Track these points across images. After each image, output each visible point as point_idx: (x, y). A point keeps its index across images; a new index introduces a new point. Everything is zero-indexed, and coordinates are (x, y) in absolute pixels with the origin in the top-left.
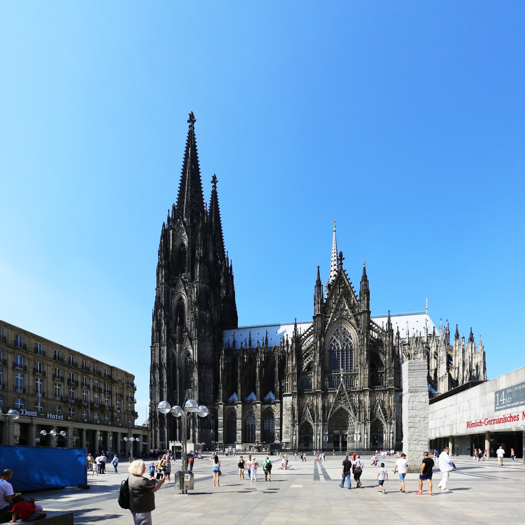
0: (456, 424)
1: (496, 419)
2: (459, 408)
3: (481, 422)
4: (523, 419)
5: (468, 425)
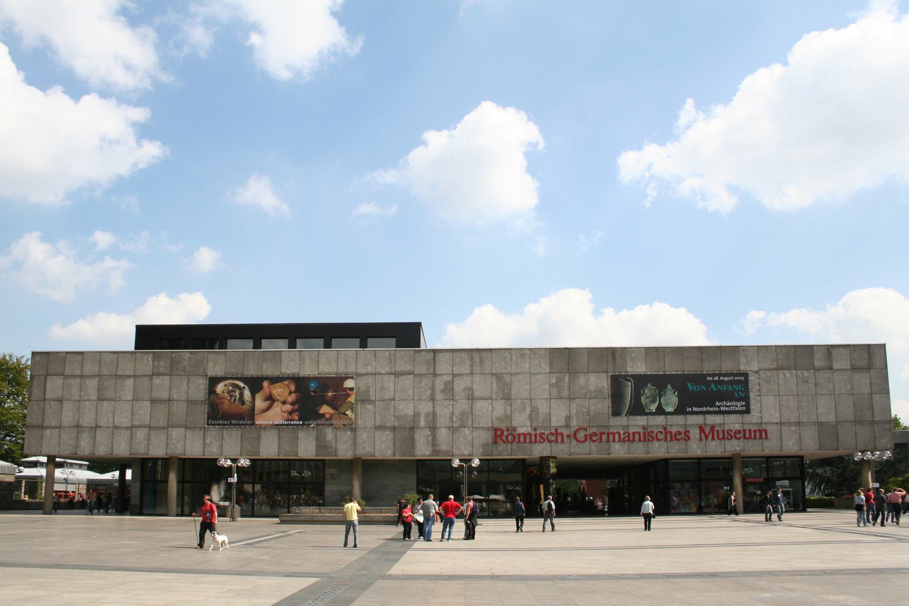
0: (433, 428)
1: (619, 434)
2: (449, 389)
3: (557, 433)
4: (701, 439)
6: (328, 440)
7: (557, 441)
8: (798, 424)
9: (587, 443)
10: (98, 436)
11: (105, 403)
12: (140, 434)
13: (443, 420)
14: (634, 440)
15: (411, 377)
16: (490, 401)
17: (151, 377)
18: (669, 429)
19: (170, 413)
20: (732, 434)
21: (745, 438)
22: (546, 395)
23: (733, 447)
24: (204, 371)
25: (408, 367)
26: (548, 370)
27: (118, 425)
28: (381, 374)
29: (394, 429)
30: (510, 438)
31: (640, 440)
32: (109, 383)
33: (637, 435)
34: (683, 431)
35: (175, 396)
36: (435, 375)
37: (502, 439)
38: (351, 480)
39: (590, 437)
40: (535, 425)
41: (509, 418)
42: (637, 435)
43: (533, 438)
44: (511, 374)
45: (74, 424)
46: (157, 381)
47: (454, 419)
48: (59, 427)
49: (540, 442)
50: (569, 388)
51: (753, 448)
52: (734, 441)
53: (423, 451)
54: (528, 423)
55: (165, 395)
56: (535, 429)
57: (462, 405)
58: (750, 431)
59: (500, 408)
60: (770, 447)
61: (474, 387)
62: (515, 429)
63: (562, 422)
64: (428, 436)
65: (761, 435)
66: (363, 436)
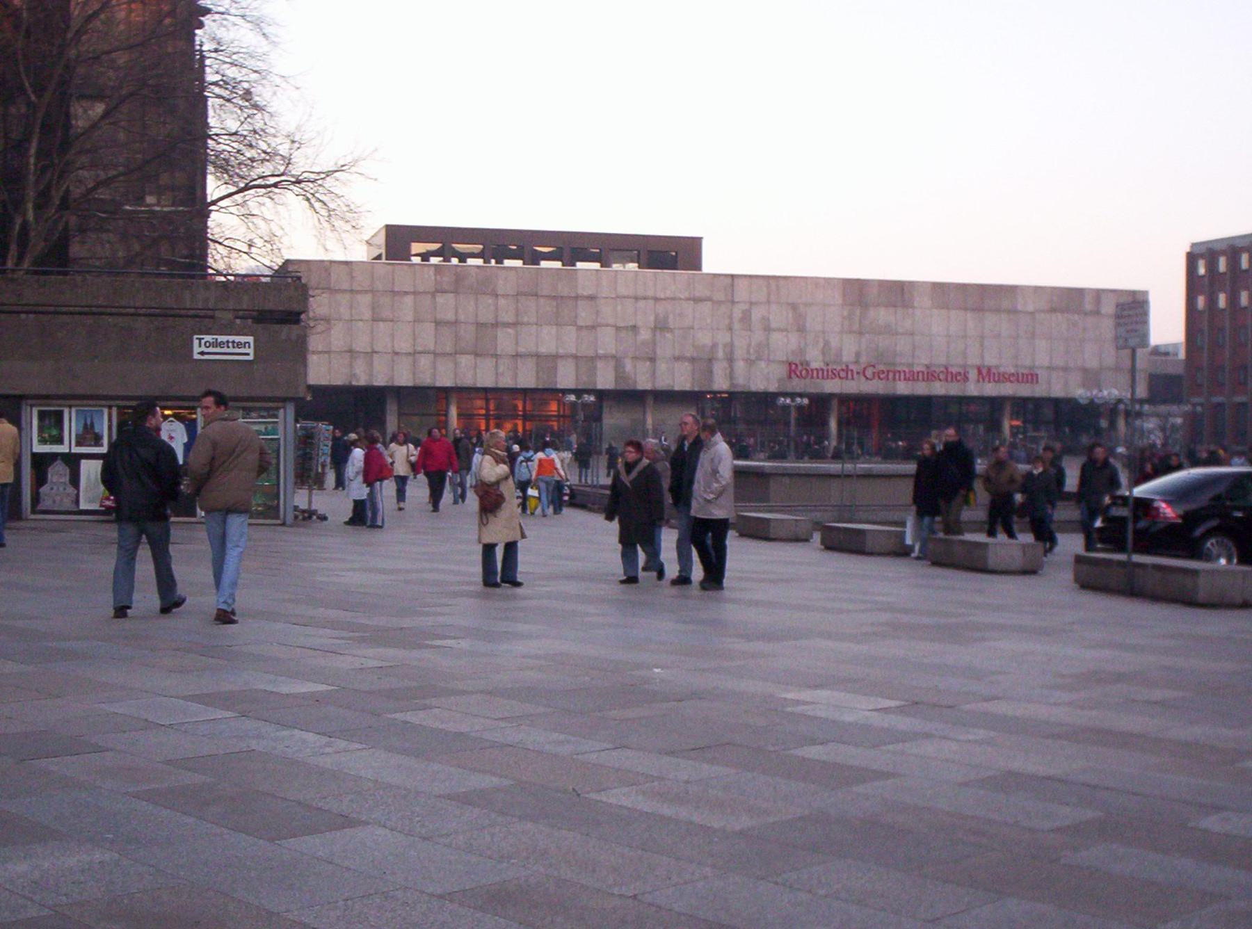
0: (731, 360)
1: (904, 371)
2: (746, 318)
3: (847, 370)
4: (978, 381)
5: (791, 371)
6: (627, 370)
7: (847, 378)
8: (1065, 369)
9: (874, 381)
10: (376, 363)
11: (381, 324)
12: (424, 361)
13: (739, 353)
14: (918, 380)
15: (709, 303)
16: (784, 333)
17: (433, 295)
18: (950, 370)
19: (457, 338)
20: (1006, 376)
21: (1018, 381)
22: (838, 328)
23: (1007, 389)
24: (493, 290)
25: (707, 293)
26: (840, 302)
27: (397, 350)
28: (681, 299)
29: (693, 360)
30: (804, 372)
31: (923, 380)
32: (385, 300)
33: (920, 375)
34: (962, 372)
35: (462, 318)
36: (733, 302)
37: (796, 374)
38: (644, 413)
39: (877, 375)
40: (827, 359)
41: (801, 351)
42: (920, 375)
43: (825, 373)
44: (806, 305)
45: (346, 349)
46: (440, 299)
47: (752, 351)
48: (328, 352)
49: (832, 378)
50: (860, 322)
51: (1024, 391)
52: (1008, 384)
53: (721, 383)
54: (821, 358)
55: (450, 316)
56: (828, 365)
57: (758, 336)
58: (1023, 374)
59: (794, 340)
60: (1039, 391)
61: (771, 318)
62: (808, 364)
63: (852, 358)
64: (726, 369)
65: (1032, 379)
66: (662, 367)
